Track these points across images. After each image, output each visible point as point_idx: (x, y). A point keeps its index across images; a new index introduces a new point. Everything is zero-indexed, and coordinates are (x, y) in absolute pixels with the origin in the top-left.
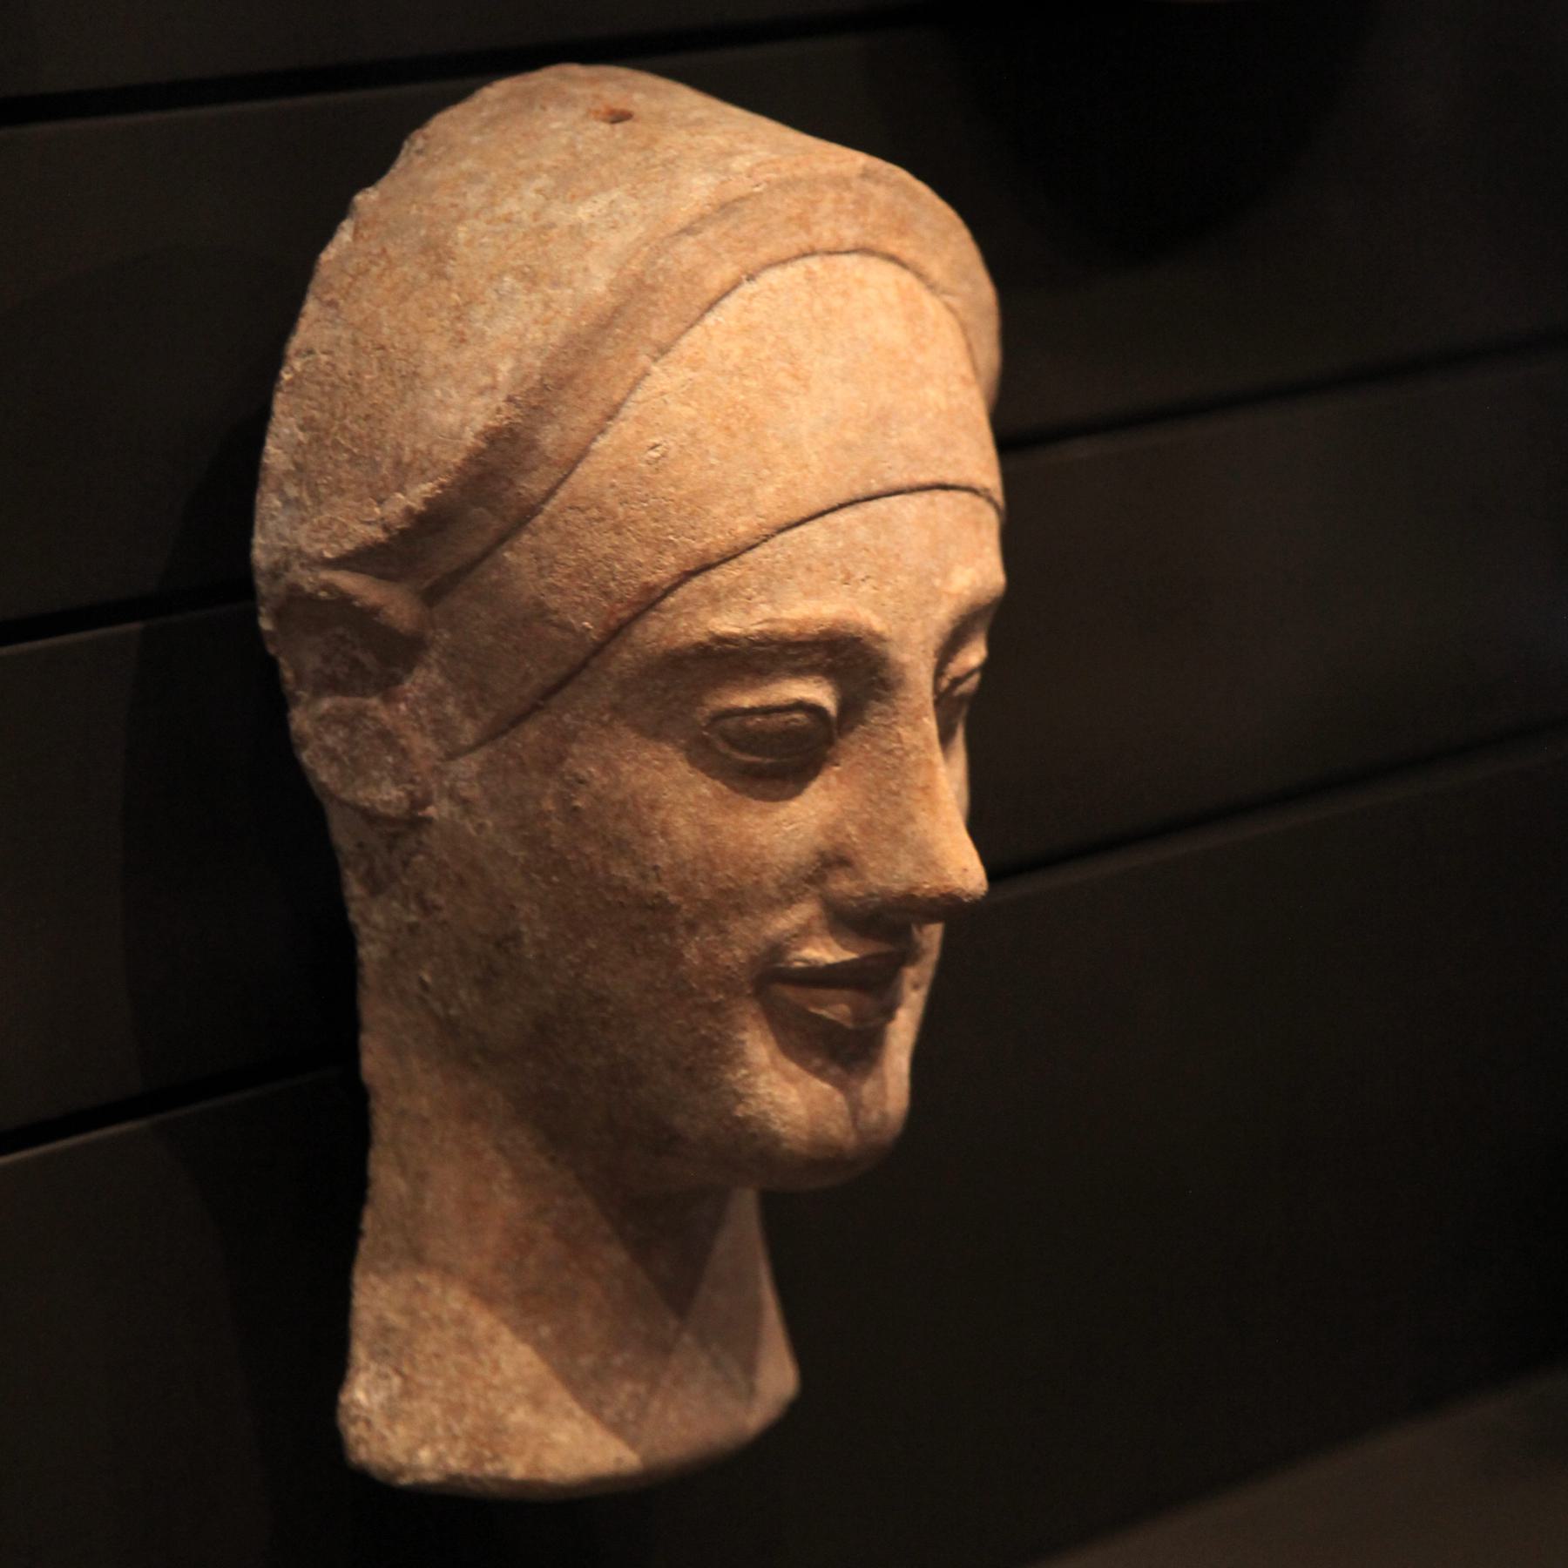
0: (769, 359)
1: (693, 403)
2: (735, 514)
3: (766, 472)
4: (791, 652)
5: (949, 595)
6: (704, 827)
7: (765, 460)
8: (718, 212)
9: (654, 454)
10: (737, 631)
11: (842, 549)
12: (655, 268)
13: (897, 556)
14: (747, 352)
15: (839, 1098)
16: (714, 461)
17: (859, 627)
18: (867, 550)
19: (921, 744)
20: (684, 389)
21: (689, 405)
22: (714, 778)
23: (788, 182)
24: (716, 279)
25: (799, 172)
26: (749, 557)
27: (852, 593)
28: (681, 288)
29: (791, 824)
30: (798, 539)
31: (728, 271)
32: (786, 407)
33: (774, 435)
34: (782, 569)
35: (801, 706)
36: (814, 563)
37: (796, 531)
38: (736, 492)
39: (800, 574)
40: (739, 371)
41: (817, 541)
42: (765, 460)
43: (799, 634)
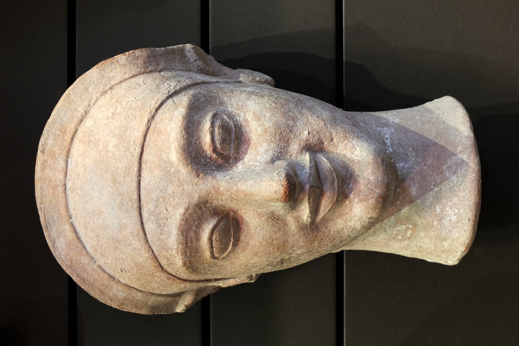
0: (94, 223)
1: (107, 256)
2: (142, 255)
3: (128, 241)
4: (189, 245)
9: (124, 271)
10: (181, 261)
16: (125, 257)
19: (229, 193)
24: (70, 235)
26: (156, 253)
30: (151, 235)
34: (161, 243)
35: (210, 239)
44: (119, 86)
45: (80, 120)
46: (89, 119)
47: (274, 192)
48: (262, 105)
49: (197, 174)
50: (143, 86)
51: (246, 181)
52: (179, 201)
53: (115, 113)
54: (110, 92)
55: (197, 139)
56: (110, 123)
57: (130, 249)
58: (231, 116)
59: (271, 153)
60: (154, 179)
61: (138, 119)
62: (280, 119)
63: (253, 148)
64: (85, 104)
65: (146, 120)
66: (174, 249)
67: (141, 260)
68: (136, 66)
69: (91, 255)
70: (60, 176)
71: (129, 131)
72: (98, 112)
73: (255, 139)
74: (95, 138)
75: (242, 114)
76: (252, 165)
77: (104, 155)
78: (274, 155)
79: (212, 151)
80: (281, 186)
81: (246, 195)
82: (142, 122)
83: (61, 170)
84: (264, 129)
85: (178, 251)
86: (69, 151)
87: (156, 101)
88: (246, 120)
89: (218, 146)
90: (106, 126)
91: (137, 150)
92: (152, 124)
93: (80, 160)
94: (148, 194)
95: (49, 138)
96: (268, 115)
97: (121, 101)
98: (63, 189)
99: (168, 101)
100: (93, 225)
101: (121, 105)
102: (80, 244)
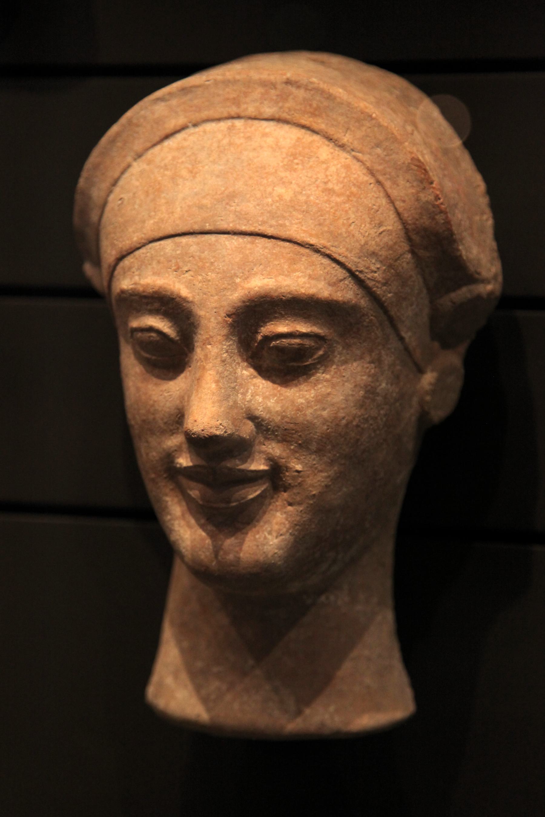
0: (182, 162)
1: (140, 180)
3: (153, 213)
4: (144, 300)
5: (243, 288)
7: (155, 208)
11: (179, 254)
13: (212, 263)
14: (174, 158)
15: (208, 541)
17: (172, 293)
19: (202, 357)
23: (229, 81)
24: (172, 124)
25: (238, 77)
26: (137, 253)
27: (177, 277)
29: (168, 392)
30: (158, 247)
31: (181, 120)
35: (151, 329)
36: (162, 259)
37: (157, 244)
39: (154, 263)
40: (166, 168)
41: (167, 249)
42: (155, 208)
43: (144, 292)
44: (382, 194)
45: (331, 137)
46: (332, 151)
47: (196, 418)
48: (343, 406)
49: (232, 315)
50: (376, 233)
51: (217, 382)
52: (197, 288)
53: (332, 194)
54: (372, 180)
55: (281, 314)
56: (318, 187)
59: (265, 415)
61: (315, 229)
62: (318, 431)
63: (275, 391)
64: (356, 144)
65: (313, 241)
66: (140, 279)
67: (131, 230)
68: (417, 216)
70: (251, 110)
71: (300, 216)
72: (339, 166)
73: (288, 394)
74: (297, 164)
75: (328, 376)
77: (270, 180)
78: (263, 420)
79: (265, 335)
80: (202, 429)
81: (199, 381)
82: (311, 235)
84: (303, 408)
85: (135, 284)
87: (343, 255)
88: (318, 381)
89: (273, 343)
90: (314, 180)
91: (270, 230)
92: (307, 251)
93: (270, 140)
94: (210, 245)
95: (308, 92)
96: (325, 413)
97: (351, 201)
98: (233, 114)
99: (344, 272)
100: (180, 161)
101: (344, 201)
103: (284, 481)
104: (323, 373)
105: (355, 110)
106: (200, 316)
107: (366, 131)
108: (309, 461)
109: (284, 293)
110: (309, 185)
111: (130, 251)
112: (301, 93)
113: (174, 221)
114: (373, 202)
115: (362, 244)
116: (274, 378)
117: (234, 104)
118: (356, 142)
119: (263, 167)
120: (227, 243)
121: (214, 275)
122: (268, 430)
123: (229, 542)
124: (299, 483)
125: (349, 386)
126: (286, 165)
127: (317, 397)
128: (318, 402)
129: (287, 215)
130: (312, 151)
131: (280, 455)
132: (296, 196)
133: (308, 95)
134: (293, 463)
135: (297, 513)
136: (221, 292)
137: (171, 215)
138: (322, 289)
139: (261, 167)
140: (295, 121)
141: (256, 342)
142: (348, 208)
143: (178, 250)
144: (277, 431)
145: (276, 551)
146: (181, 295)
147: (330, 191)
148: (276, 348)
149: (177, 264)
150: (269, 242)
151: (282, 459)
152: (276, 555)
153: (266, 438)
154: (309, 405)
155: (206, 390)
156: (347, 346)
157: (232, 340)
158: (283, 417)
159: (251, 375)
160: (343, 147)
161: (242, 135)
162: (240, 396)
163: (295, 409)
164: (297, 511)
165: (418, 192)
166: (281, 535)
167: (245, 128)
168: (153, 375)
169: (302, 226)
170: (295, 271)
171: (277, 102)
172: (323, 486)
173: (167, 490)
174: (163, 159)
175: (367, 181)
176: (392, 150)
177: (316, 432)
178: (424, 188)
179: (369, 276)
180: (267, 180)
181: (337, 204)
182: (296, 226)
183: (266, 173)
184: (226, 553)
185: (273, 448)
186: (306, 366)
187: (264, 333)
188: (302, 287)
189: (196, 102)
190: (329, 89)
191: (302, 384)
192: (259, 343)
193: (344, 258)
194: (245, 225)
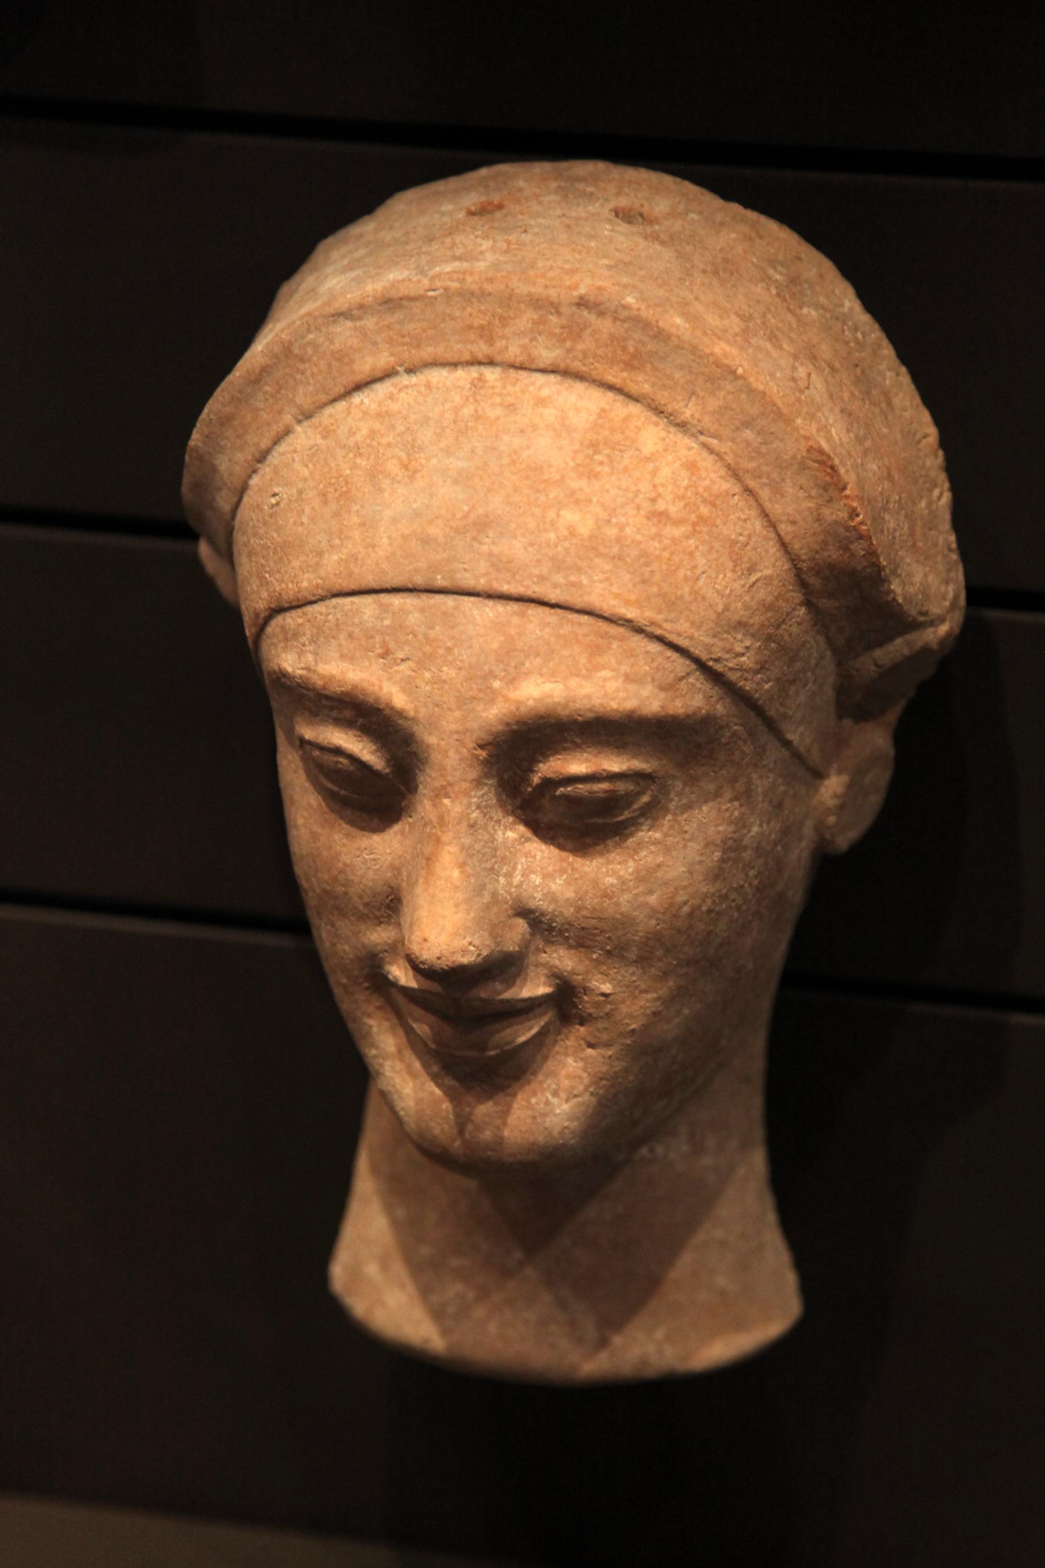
0: (389, 445)
1: (310, 466)
3: (337, 541)
4: (324, 702)
5: (507, 700)
6: (311, 832)
7: (341, 532)
8: (380, 305)
11: (387, 627)
12: (305, 341)
13: (449, 650)
14: (372, 433)
15: (446, 1106)
16: (305, 520)
17: (377, 700)
18: (415, 636)
19: (435, 820)
20: (310, 452)
21: (307, 466)
22: (319, 793)
24: (366, 365)
25: (489, 287)
26: (309, 609)
27: (385, 668)
28: (330, 365)
29: (371, 854)
30: (349, 607)
31: (384, 360)
32: (381, 491)
33: (358, 511)
34: (330, 629)
35: (338, 751)
36: (357, 631)
38: (311, 552)
39: (342, 636)
41: (364, 613)
44: (753, 513)
45: (662, 408)
46: (663, 434)
47: (426, 935)
48: (685, 883)
49: (486, 745)
50: (744, 586)
51: (462, 865)
54: (737, 489)
56: (638, 508)
57: (320, 542)
58: (652, 812)
59: (545, 905)
60: (478, 635)
62: (640, 928)
63: (565, 865)
64: (707, 422)
65: (631, 613)
67: (296, 563)
68: (816, 547)
69: (315, 413)
70: (514, 351)
71: (607, 567)
72: (677, 464)
73: (587, 869)
74: (601, 463)
75: (658, 835)
76: (515, 864)
77: (552, 496)
78: (542, 914)
80: (438, 955)
82: (627, 603)
83: (529, 355)
84: (613, 892)
85: (308, 669)
86: (580, 377)
87: (685, 635)
88: (640, 845)
89: (561, 790)
90: (631, 495)
92: (622, 630)
93: (550, 414)
94: (444, 614)
95: (618, 323)
96: (653, 900)
97: (700, 532)
98: (480, 356)
99: (688, 662)
100: (384, 441)
102: (342, 390)
103: (580, 1009)
104: (649, 830)
105: (705, 361)
106: (428, 746)
107: (724, 398)
108: (625, 976)
109: (580, 709)
110: (625, 504)
111: (294, 604)
112: (606, 325)
113: (377, 564)
114: (738, 529)
115: (720, 610)
116: (562, 840)
117: (481, 336)
118: (706, 419)
119: (539, 469)
120: (475, 612)
121: (453, 673)
122: (551, 929)
123: (484, 1110)
124: (607, 1014)
125: (694, 847)
126: (580, 465)
127: (637, 872)
128: (640, 881)
129: (585, 564)
130: (627, 438)
131: (573, 969)
132: (599, 528)
133: (619, 329)
134: (596, 981)
135: (602, 1060)
136: (465, 704)
137: (370, 550)
138: (648, 698)
139: (536, 469)
140: (598, 378)
141: (530, 785)
142: (694, 546)
143: (385, 618)
144: (567, 930)
145: (566, 1124)
146: (394, 704)
147: (661, 517)
148: (566, 797)
149: (384, 644)
150: (551, 614)
151: (577, 975)
152: (566, 1131)
153: (549, 942)
154: (624, 888)
155: (442, 882)
156: (692, 781)
157: (487, 784)
158: (579, 909)
159: (522, 836)
160: (683, 427)
161: (498, 400)
162: (502, 880)
163: (599, 894)
164: (604, 1057)
165: (819, 507)
166: (575, 1096)
167: (504, 387)
168: (342, 818)
169: (612, 585)
170: (597, 668)
171: (562, 341)
172: (648, 1015)
173: (371, 1009)
174: (352, 433)
175: (727, 492)
176: (772, 433)
177: (637, 931)
178: (830, 500)
179: (731, 665)
180: (547, 495)
181: (674, 540)
182: (600, 586)
183: (545, 481)
184: (478, 1129)
185: (559, 959)
186: (619, 823)
187: (545, 774)
188: (614, 699)
189: (410, 327)
190: (657, 322)
191: (612, 852)
192: (534, 789)
193: (687, 640)
194: (508, 583)
